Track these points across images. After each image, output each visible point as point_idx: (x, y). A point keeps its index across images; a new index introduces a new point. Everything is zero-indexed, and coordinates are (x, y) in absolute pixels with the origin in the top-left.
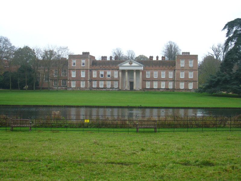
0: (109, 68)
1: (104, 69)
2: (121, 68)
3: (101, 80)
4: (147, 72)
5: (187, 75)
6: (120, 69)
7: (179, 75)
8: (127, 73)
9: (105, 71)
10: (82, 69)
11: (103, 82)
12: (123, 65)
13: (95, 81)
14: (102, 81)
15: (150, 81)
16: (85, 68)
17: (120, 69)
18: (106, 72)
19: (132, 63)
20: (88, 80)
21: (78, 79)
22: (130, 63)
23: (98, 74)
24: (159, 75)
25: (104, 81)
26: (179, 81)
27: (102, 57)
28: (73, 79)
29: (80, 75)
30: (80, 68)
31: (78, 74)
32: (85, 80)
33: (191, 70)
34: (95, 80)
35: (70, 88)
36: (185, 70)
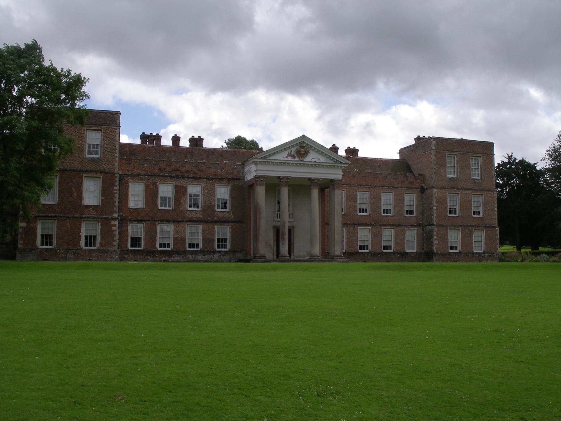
0: (195, 171)
1: (177, 177)
3: (162, 221)
5: (466, 204)
7: (442, 202)
8: (285, 191)
9: (181, 182)
10: (86, 171)
11: (169, 228)
13: (140, 221)
14: (168, 221)
19: (306, 153)
20: (115, 219)
21: (71, 209)
23: (151, 194)
24: (376, 201)
25: (175, 221)
26: (447, 226)
27: (144, 137)
28: (48, 213)
29: (80, 197)
32: (100, 213)
33: (478, 188)
34: (138, 216)
35: (32, 250)
36: (462, 189)
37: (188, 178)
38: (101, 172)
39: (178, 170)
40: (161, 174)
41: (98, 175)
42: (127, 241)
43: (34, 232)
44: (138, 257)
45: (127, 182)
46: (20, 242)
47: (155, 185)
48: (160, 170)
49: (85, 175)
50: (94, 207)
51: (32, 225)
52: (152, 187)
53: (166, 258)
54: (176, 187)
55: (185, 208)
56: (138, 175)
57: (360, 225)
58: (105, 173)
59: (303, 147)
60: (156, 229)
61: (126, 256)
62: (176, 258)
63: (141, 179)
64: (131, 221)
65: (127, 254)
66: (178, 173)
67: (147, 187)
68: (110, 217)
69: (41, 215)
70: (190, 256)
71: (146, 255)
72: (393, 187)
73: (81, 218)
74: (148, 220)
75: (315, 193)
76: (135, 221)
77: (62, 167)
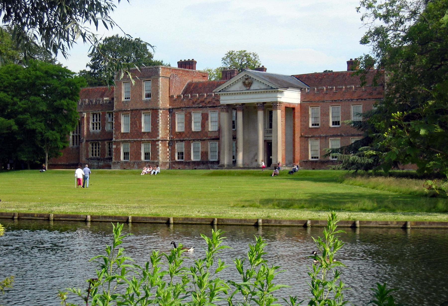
0: (214, 101)
2: (225, 100)
4: (310, 109)
6: (222, 102)
8: (240, 115)
9: (205, 111)
11: (200, 144)
12: (230, 89)
13: (182, 141)
15: (320, 137)
16: (150, 106)
17: (222, 102)
18: (207, 115)
20: (158, 140)
21: (136, 135)
22: (244, 83)
25: (201, 140)
30: (139, 106)
31: (135, 124)
35: (118, 162)
37: (210, 107)
38: (151, 109)
39: (204, 101)
40: (194, 106)
41: (149, 112)
42: (175, 155)
43: (118, 150)
44: (180, 166)
45: (174, 114)
46: (113, 158)
47: (190, 113)
48: (193, 103)
49: (143, 112)
50: (148, 133)
51: (118, 147)
52: (188, 115)
53: (196, 167)
54: (202, 114)
55: (208, 129)
56: (180, 108)
57: (331, 136)
58: (153, 109)
59: (246, 79)
60: (191, 146)
61: (174, 166)
62: (202, 166)
63: (183, 111)
64: (177, 141)
65: (174, 164)
66: (203, 104)
67: (186, 115)
68: (155, 139)
69: (122, 140)
70: (210, 165)
71: (185, 165)
72: (362, 99)
73: (141, 141)
74: (186, 140)
75: (260, 114)
76: (179, 141)
77: (132, 108)
